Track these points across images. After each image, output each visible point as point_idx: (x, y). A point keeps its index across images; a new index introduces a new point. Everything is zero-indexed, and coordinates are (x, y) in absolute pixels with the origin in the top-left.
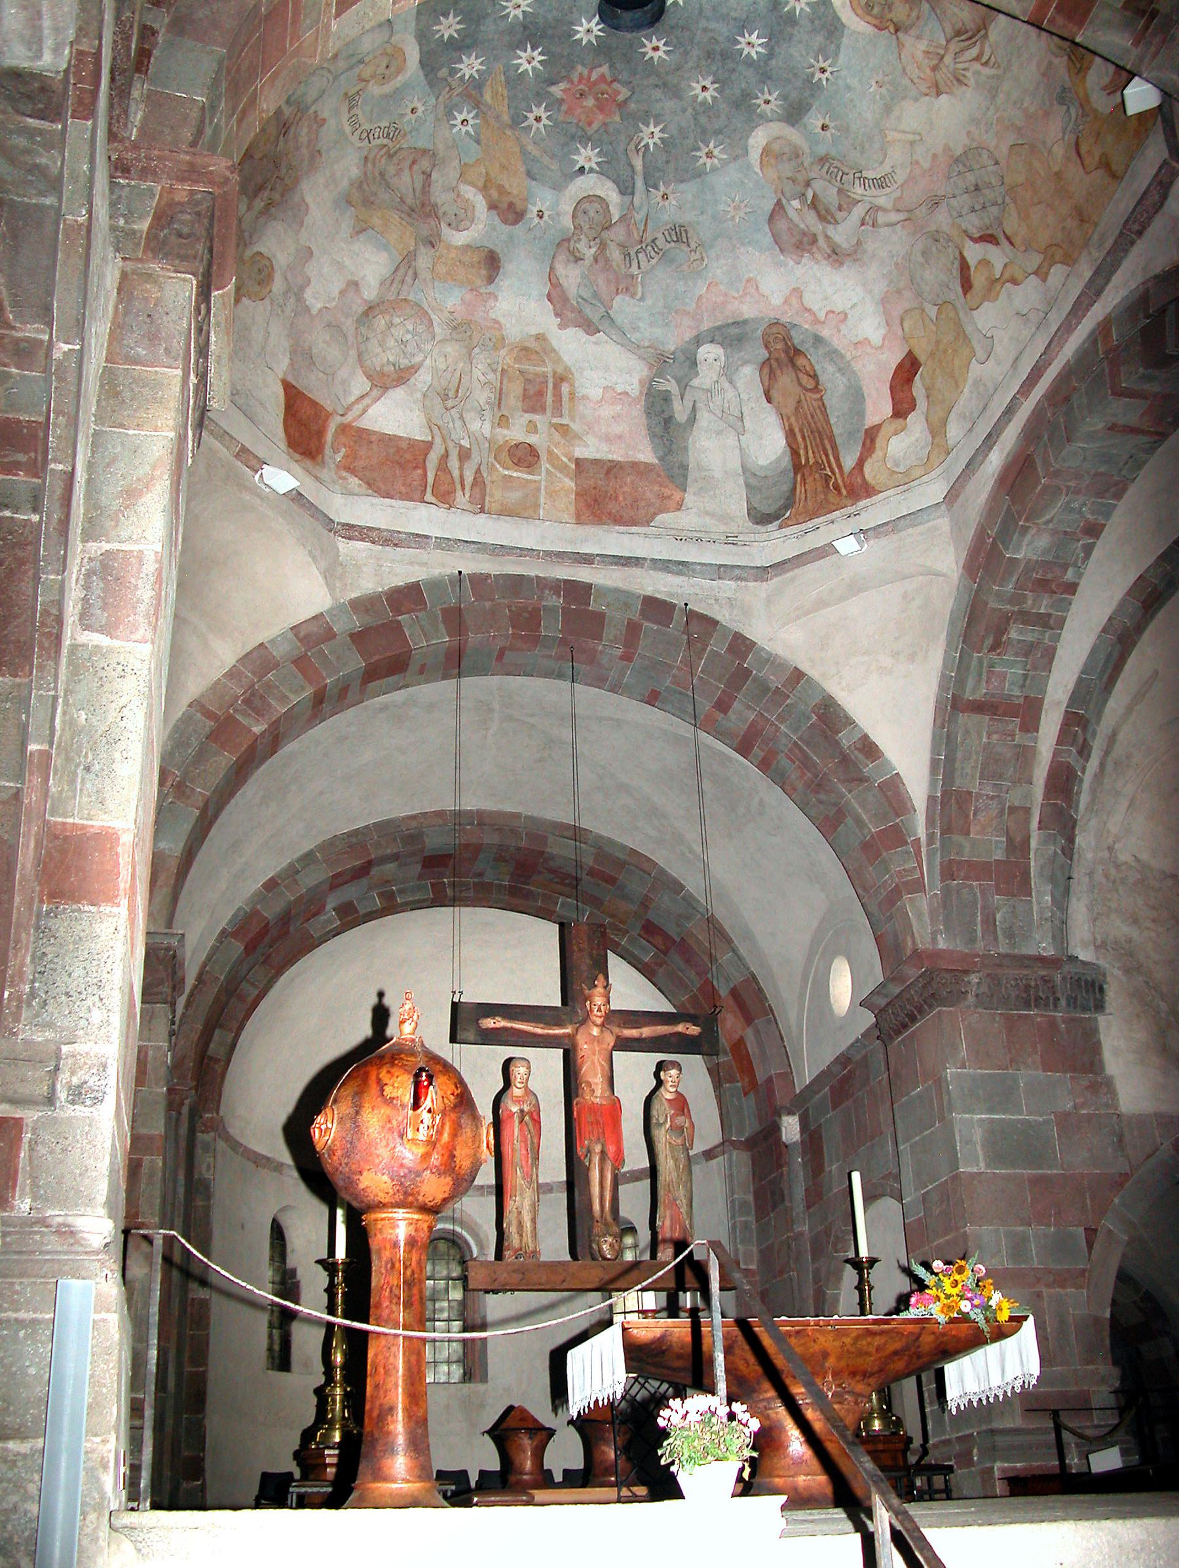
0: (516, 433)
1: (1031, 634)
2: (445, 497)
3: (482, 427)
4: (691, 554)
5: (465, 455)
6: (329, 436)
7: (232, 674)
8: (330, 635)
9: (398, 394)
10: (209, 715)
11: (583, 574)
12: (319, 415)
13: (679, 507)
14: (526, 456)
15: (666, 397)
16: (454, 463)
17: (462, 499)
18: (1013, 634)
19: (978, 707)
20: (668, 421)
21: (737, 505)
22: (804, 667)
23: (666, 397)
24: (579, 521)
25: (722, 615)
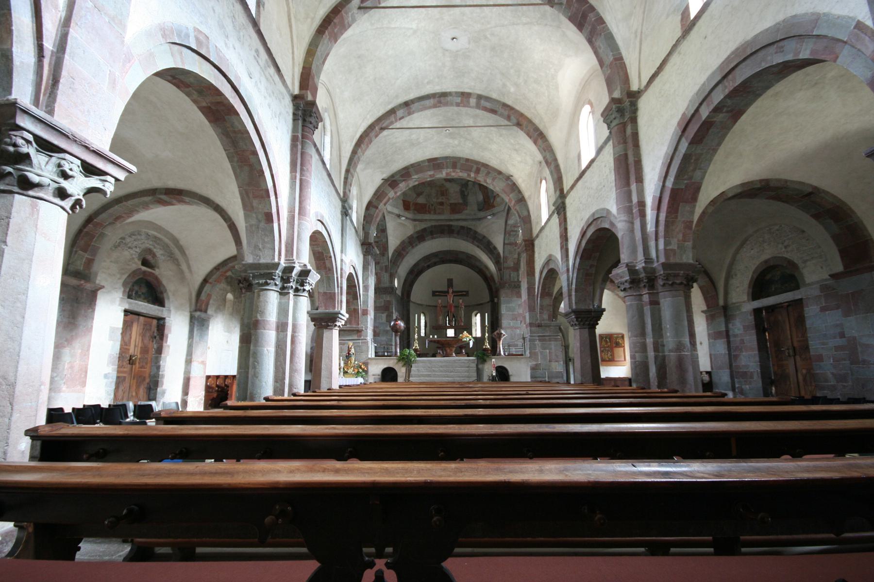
0: (440, 200)
1: (514, 233)
2: (430, 213)
3: (435, 200)
4: (468, 217)
5: (432, 205)
6: (411, 205)
7: (400, 245)
8: (413, 237)
9: (421, 196)
10: (397, 252)
11: (451, 223)
12: (409, 202)
13: (466, 209)
14: (442, 204)
15: (463, 192)
16: (431, 207)
17: (432, 212)
18: (512, 233)
19: (507, 244)
20: (464, 195)
21: (475, 207)
22: (486, 235)
23: (463, 192)
24: (451, 214)
25: (472, 228)
